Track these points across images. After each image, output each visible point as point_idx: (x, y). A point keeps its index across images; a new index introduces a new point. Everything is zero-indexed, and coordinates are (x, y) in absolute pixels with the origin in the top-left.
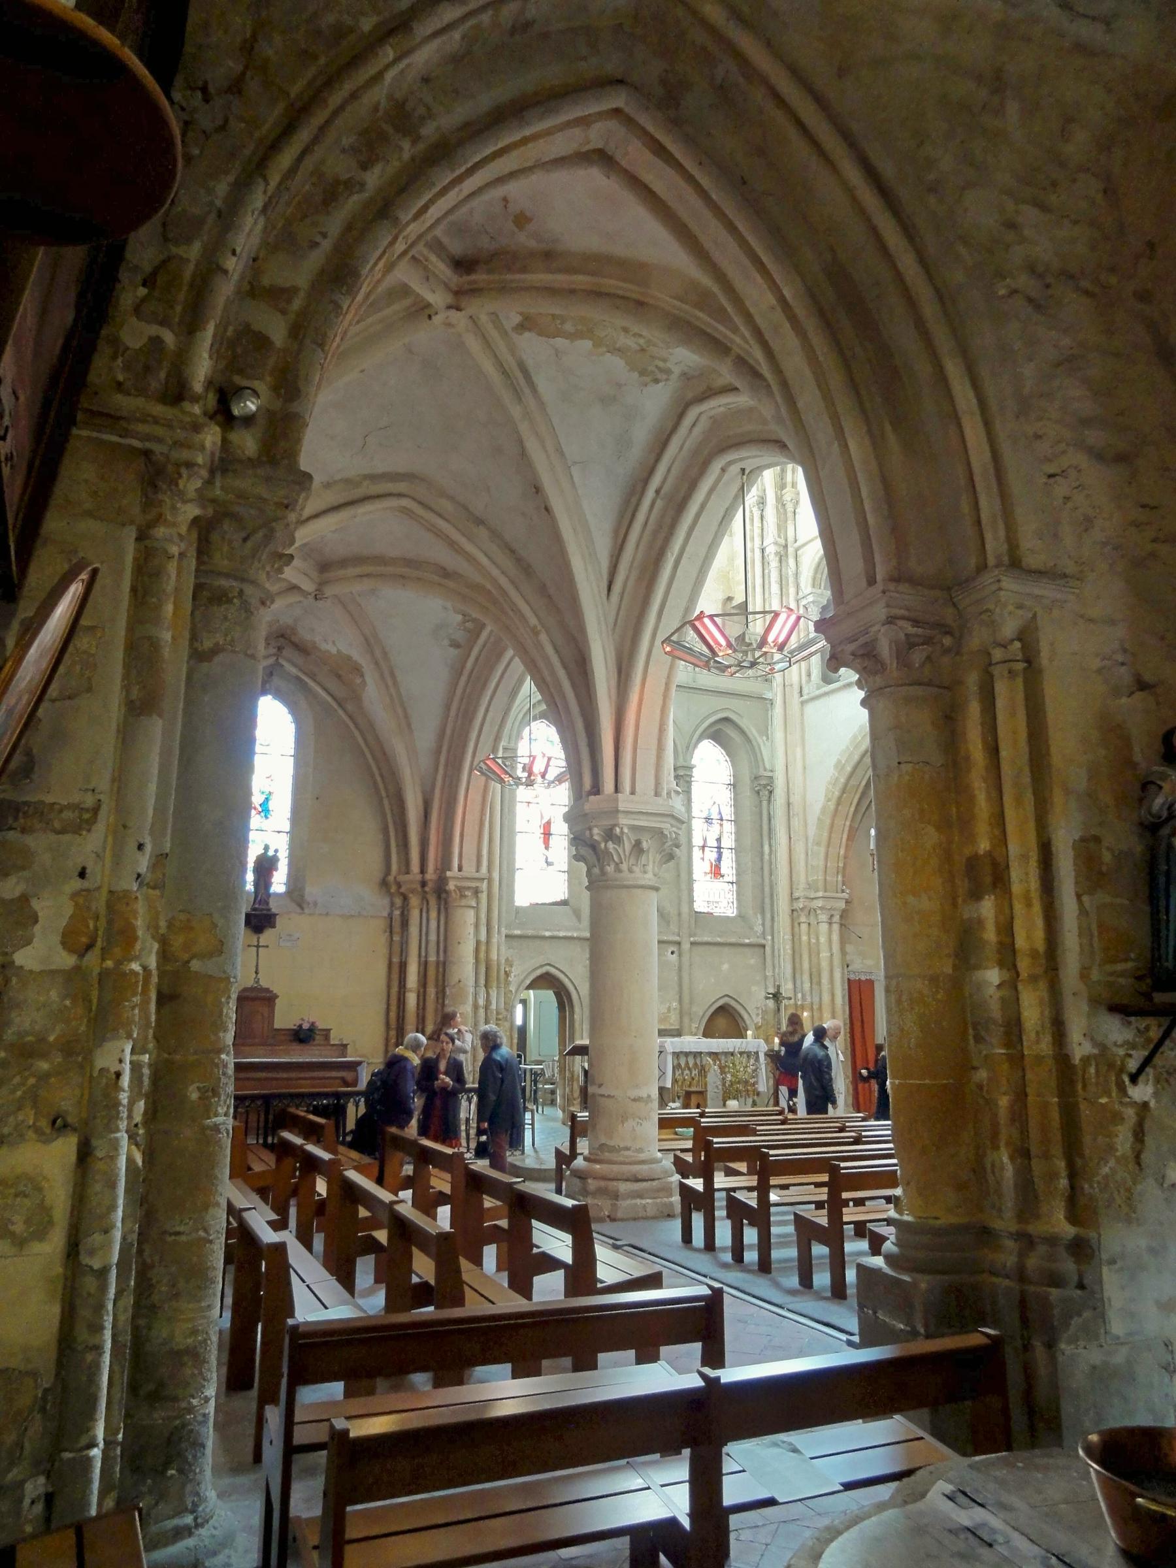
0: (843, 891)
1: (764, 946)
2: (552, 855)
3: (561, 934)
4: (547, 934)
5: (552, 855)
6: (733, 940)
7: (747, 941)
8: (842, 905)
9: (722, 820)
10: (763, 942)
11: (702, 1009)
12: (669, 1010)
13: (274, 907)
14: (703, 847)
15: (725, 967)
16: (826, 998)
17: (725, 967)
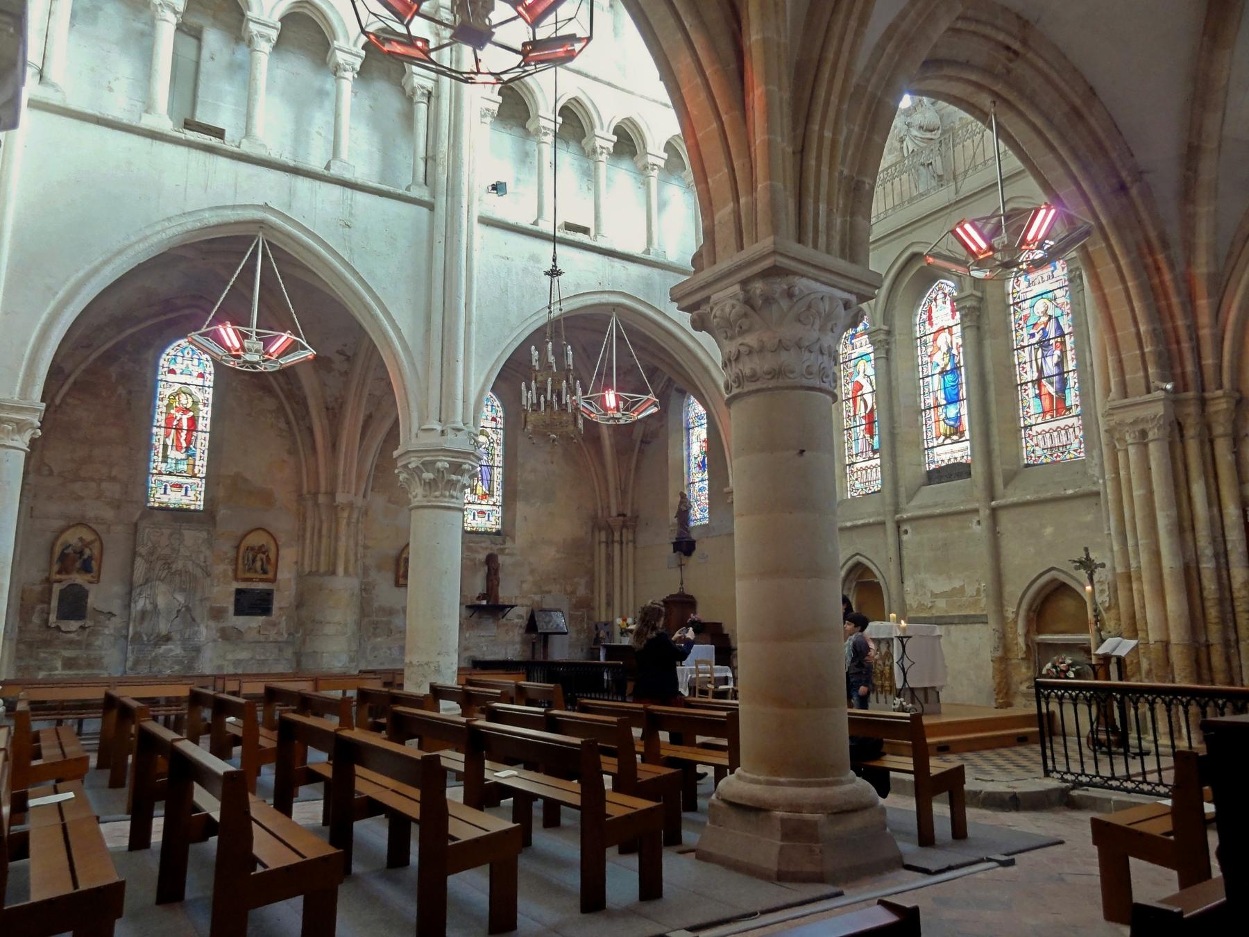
0: (1158, 389)
1: (1097, 494)
3: (860, 522)
4: (849, 524)
6: (1049, 495)
7: (1070, 492)
8: (1159, 409)
9: (1063, 335)
10: (1095, 489)
11: (1017, 588)
12: (978, 591)
13: (694, 536)
14: (1038, 383)
15: (1049, 530)
16: (1144, 558)
17: (1049, 530)
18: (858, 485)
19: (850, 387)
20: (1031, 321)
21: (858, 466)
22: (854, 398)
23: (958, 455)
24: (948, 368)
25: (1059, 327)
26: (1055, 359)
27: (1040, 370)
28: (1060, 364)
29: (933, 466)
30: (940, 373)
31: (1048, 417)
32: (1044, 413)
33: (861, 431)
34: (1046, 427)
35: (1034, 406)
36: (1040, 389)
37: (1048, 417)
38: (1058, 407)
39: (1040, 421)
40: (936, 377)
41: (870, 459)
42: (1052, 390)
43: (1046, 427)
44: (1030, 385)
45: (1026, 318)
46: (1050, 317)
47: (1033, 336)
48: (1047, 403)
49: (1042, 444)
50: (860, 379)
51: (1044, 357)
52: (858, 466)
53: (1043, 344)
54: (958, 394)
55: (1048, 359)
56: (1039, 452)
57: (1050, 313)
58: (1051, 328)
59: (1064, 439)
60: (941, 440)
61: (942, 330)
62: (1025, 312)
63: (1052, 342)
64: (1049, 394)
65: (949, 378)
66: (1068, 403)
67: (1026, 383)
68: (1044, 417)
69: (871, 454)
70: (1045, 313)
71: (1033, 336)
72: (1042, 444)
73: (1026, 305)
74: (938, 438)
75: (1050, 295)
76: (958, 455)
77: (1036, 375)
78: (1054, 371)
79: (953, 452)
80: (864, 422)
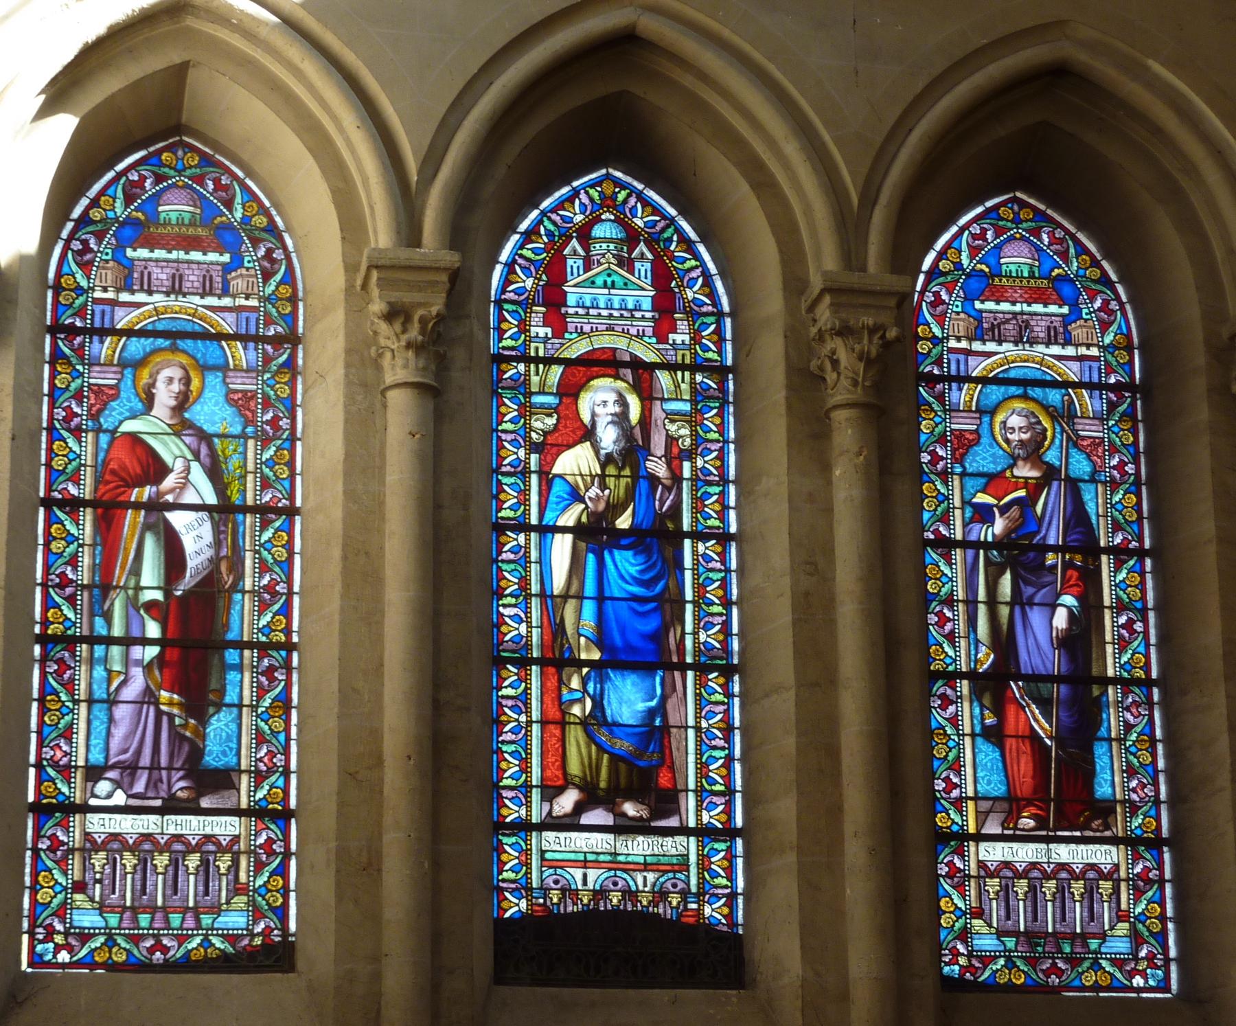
2: (222, 737)
5: (222, 737)
9: (1091, 550)
18: (87, 919)
19: (86, 450)
20: (983, 459)
21: (98, 825)
22: (108, 512)
23: (644, 881)
24: (624, 522)
25: (1078, 518)
26: (1060, 620)
27: (1004, 643)
28: (1080, 640)
29: (516, 906)
30: (578, 531)
31: (1027, 822)
32: (1011, 805)
33: (131, 671)
34: (1024, 853)
35: (980, 771)
36: (999, 711)
37: (1027, 822)
38: (1059, 795)
39: (993, 828)
40: (562, 546)
41: (172, 807)
42: (1042, 727)
43: (1024, 853)
44: (964, 686)
45: (963, 444)
46: (1050, 474)
47: (983, 514)
48: (1025, 767)
49: (995, 910)
50: (151, 426)
51: (1017, 599)
52: (98, 825)
53: (1019, 553)
54: (658, 638)
55: (1036, 616)
56: (986, 942)
57: (1052, 456)
58: (1049, 503)
59: (1078, 911)
60: (566, 802)
61: (603, 363)
62: (964, 424)
63: (1051, 559)
64: (1033, 736)
65: (625, 565)
66: (1103, 790)
67: (952, 677)
68: (1011, 818)
69: (180, 786)
70: (1033, 450)
71: (983, 514)
72: (995, 910)
73: (962, 396)
74: (551, 792)
75: (1054, 396)
76: (644, 881)
77: (986, 657)
78: (1054, 662)
79: (614, 863)
80: (153, 630)
